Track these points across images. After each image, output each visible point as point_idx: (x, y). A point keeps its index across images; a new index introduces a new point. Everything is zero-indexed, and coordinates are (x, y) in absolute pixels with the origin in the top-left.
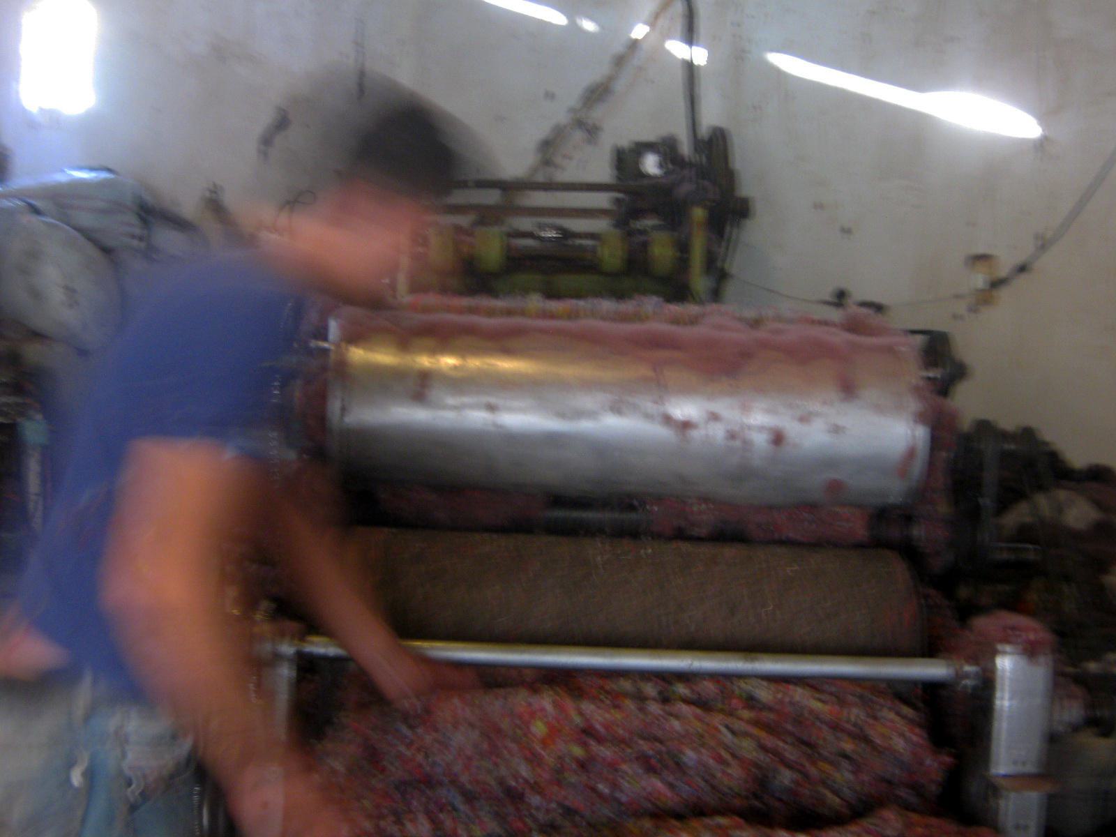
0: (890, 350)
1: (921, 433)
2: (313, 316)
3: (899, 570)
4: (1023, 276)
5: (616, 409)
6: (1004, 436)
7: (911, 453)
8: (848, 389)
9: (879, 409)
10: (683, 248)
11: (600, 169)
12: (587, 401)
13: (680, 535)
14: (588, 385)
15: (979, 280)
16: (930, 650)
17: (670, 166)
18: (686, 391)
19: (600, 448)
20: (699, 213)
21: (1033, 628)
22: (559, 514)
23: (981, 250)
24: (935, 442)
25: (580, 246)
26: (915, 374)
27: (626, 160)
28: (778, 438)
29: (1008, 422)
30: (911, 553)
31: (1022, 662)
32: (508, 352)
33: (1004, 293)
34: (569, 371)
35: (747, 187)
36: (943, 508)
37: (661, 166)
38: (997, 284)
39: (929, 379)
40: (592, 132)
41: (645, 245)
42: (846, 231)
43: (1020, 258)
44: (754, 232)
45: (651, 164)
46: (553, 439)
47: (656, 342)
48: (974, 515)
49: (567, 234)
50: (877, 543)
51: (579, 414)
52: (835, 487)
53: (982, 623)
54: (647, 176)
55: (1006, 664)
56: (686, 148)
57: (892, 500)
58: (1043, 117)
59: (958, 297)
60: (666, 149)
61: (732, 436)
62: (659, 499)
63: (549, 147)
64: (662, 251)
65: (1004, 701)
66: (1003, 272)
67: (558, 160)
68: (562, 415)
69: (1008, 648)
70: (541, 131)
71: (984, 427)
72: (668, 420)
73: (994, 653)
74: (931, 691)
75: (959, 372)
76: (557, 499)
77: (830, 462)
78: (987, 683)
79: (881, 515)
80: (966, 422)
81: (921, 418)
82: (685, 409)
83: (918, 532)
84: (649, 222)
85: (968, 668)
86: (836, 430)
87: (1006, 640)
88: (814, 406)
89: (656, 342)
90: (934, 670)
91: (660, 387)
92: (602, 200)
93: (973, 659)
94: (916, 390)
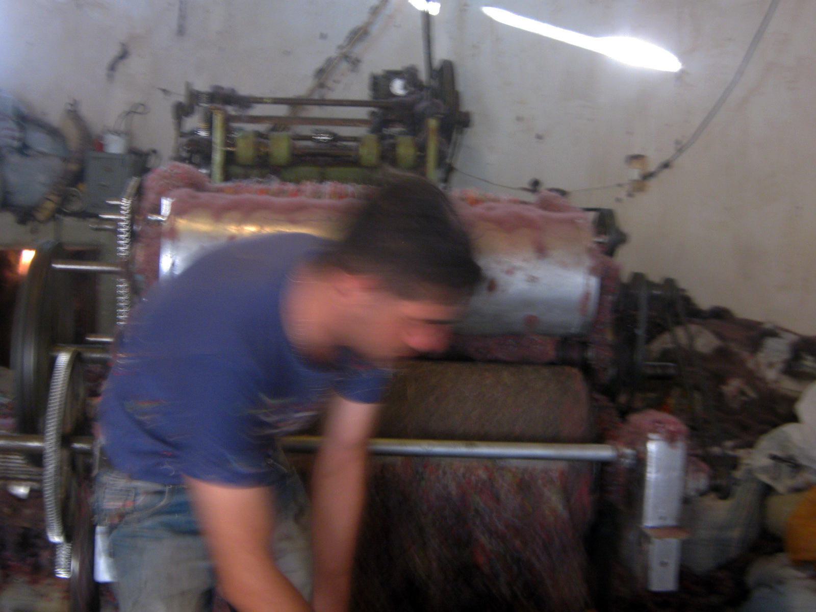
0: (572, 222)
2: (150, 196)
3: (577, 382)
4: (666, 172)
6: (652, 285)
7: (586, 296)
8: (541, 251)
9: (564, 265)
10: (422, 148)
11: (362, 91)
15: (635, 173)
16: (599, 439)
17: (413, 89)
20: (433, 123)
21: (674, 423)
24: (604, 289)
25: (345, 146)
26: (590, 239)
27: (380, 84)
29: (655, 276)
30: (586, 369)
33: (653, 183)
35: (468, 105)
36: (609, 337)
37: (405, 88)
38: (647, 176)
39: (599, 243)
40: (355, 63)
41: (393, 147)
42: (539, 137)
43: (664, 158)
44: (473, 137)
45: (398, 87)
48: (630, 341)
49: (336, 138)
50: (562, 362)
52: (531, 321)
53: (635, 419)
54: (394, 96)
55: (653, 447)
56: (423, 76)
57: (573, 330)
58: (682, 56)
59: (620, 185)
60: (409, 75)
63: (322, 74)
65: (652, 474)
66: (652, 167)
67: (330, 84)
70: (318, 62)
71: (638, 278)
73: (647, 440)
75: (621, 239)
77: (527, 302)
78: (641, 461)
79: (566, 341)
80: (625, 277)
81: (593, 271)
83: (590, 354)
84: (396, 130)
85: (628, 451)
87: (654, 431)
90: (603, 452)
92: (362, 113)
93: (631, 444)
94: (590, 251)
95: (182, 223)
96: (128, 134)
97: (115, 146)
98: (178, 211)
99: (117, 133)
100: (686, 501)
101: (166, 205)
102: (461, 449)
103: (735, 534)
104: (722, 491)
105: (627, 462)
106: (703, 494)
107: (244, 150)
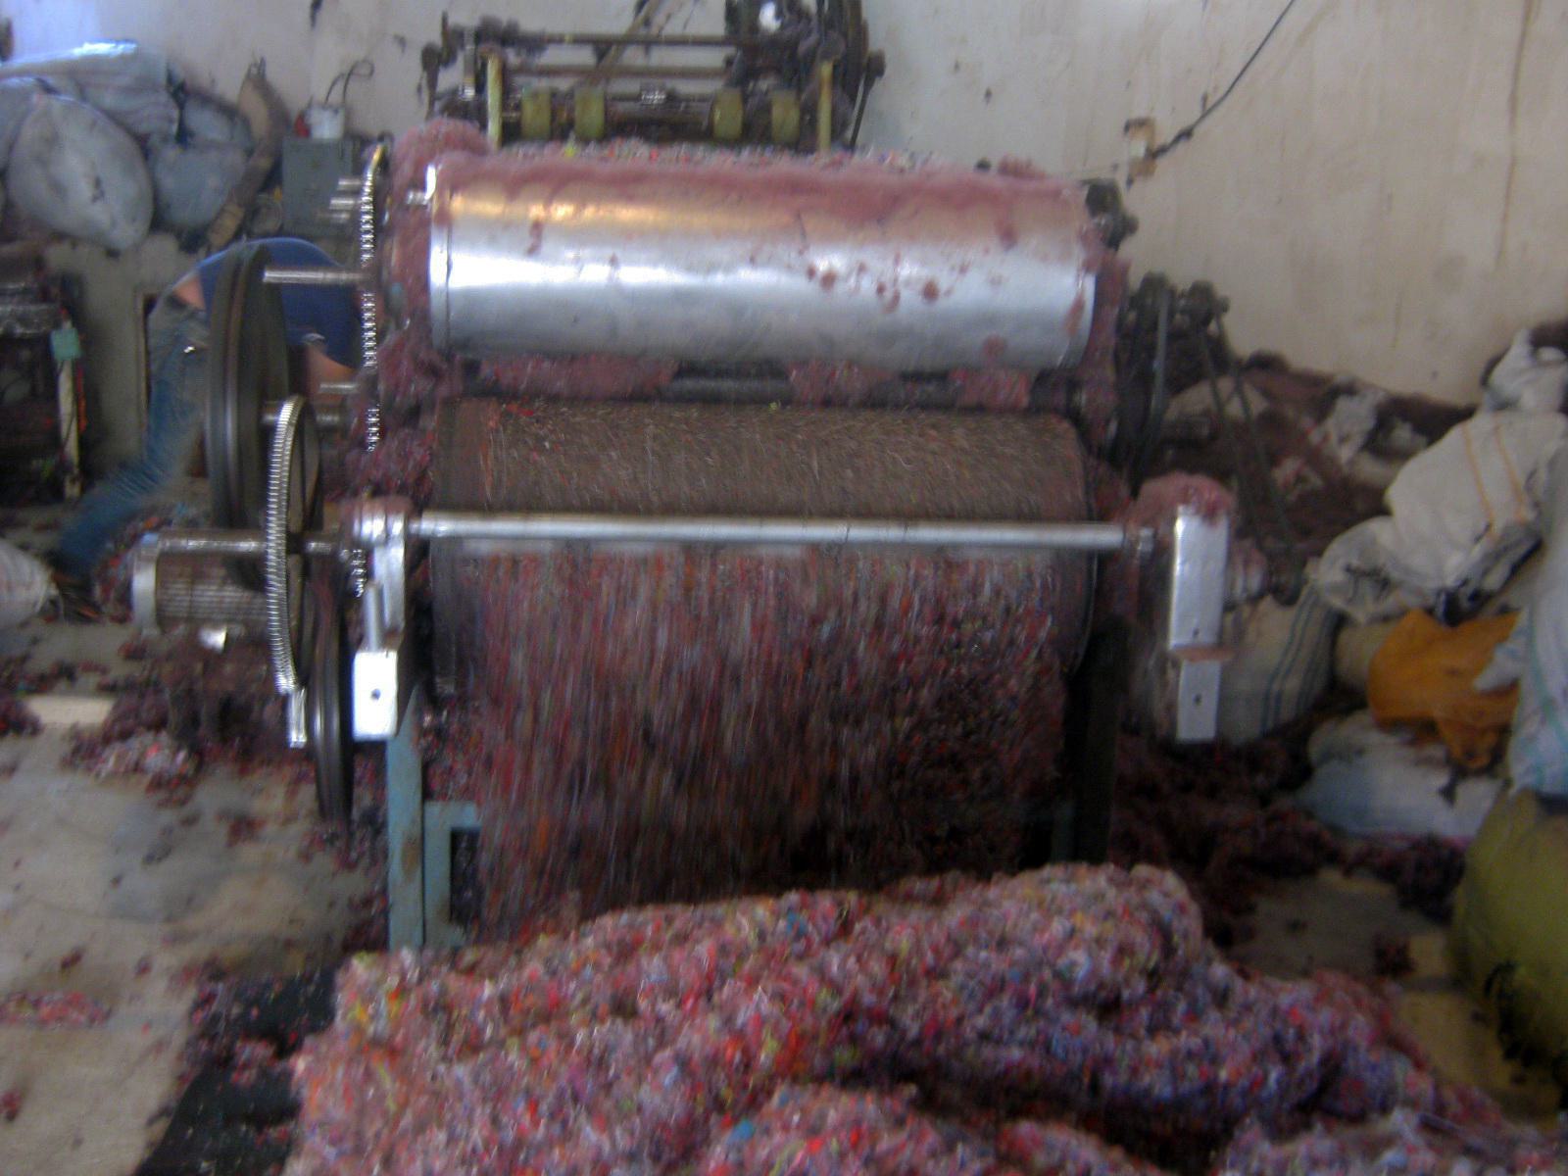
0: (1055, 194)
1: (1089, 285)
2: (406, 169)
3: (1066, 442)
4: (1181, 147)
5: (753, 261)
7: (1078, 306)
8: (1009, 237)
9: (1044, 258)
10: (809, 111)
12: (721, 252)
13: (827, 403)
14: (718, 235)
15: (1139, 148)
16: (1099, 514)
18: (830, 240)
19: (735, 306)
22: (689, 384)
23: (1138, 112)
26: (1081, 220)
28: (930, 292)
29: (1182, 278)
30: (1075, 417)
31: (1196, 522)
32: (629, 198)
33: (1162, 163)
34: (700, 220)
36: (1109, 373)
38: (1154, 154)
41: (766, 108)
46: (681, 296)
47: (794, 188)
51: (711, 268)
52: (994, 348)
53: (1152, 488)
55: (1180, 526)
61: (881, 290)
62: (802, 364)
64: (784, 113)
65: (1178, 568)
68: (690, 269)
69: (1181, 509)
71: (1154, 284)
72: (811, 273)
74: (1103, 560)
76: (688, 368)
77: (988, 318)
78: (1163, 550)
80: (1135, 281)
82: (830, 260)
83: (1082, 398)
85: (1146, 533)
86: (995, 282)
87: (1185, 501)
88: (973, 254)
89: (794, 188)
90: (1106, 536)
91: (800, 234)
93: (1145, 524)
94: (1084, 238)
95: (458, 204)
96: (346, 110)
97: (327, 128)
98: (452, 184)
99: (325, 105)
100: (1229, 606)
101: (431, 175)
102: (892, 533)
103: (1293, 685)
104: (1286, 596)
105: (1143, 547)
106: (1255, 600)
107: (534, 115)
